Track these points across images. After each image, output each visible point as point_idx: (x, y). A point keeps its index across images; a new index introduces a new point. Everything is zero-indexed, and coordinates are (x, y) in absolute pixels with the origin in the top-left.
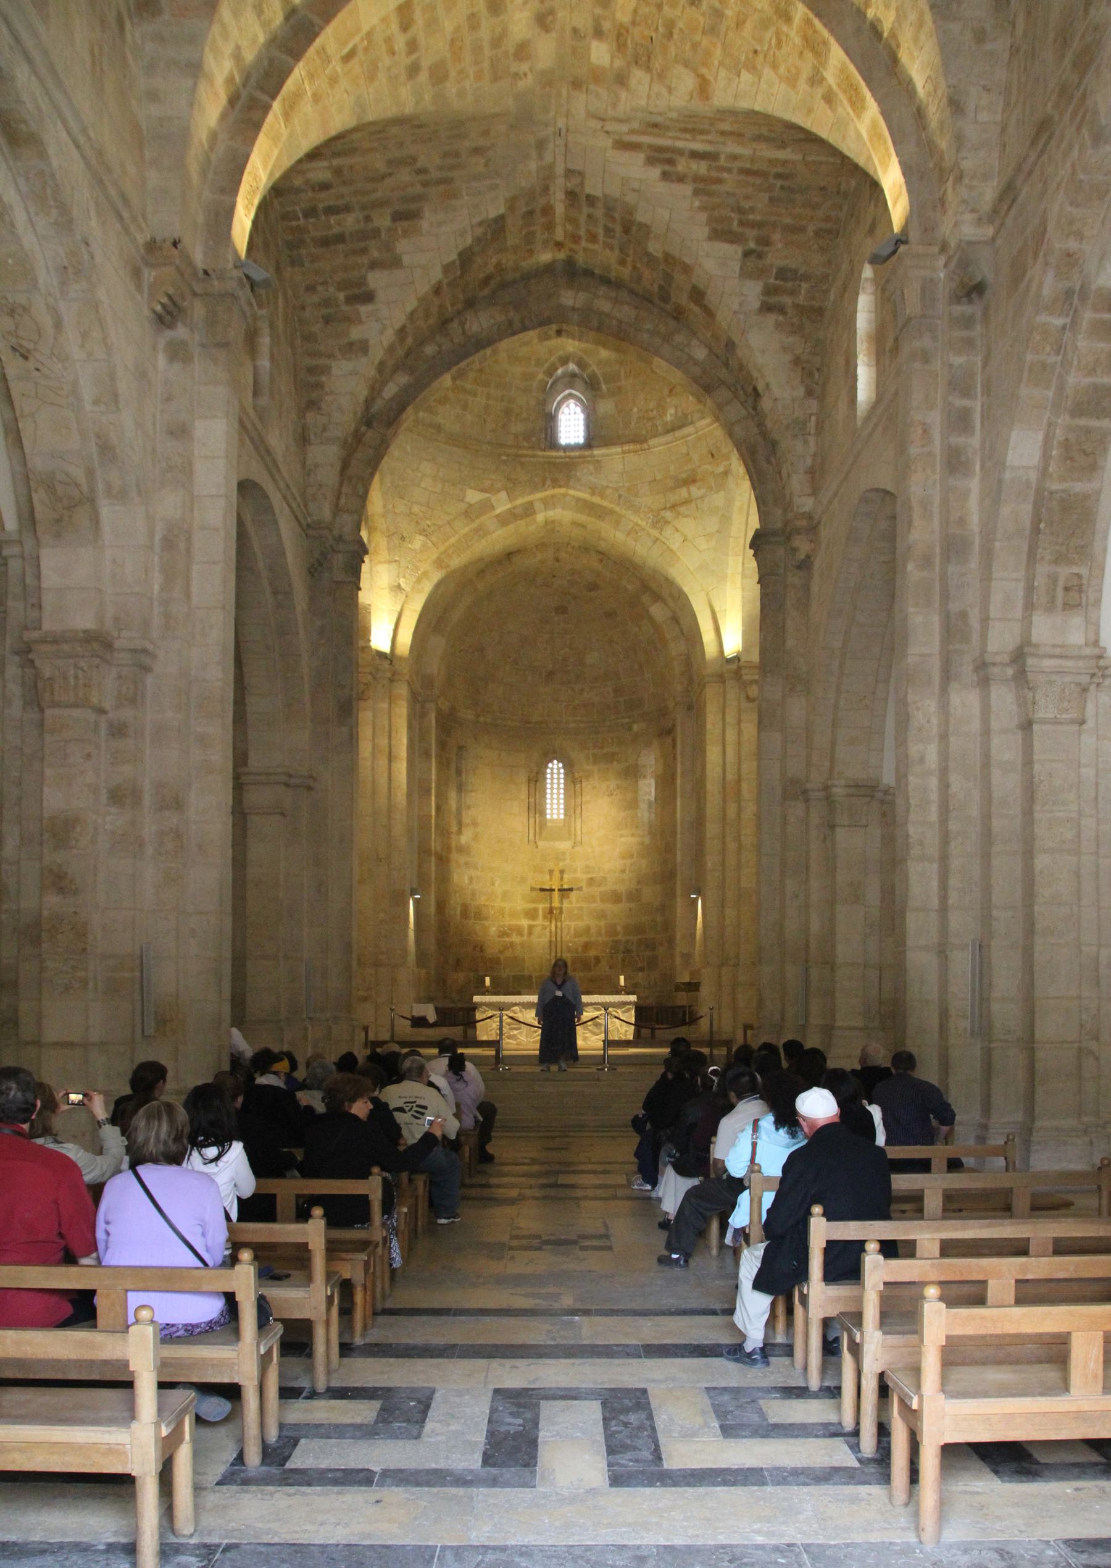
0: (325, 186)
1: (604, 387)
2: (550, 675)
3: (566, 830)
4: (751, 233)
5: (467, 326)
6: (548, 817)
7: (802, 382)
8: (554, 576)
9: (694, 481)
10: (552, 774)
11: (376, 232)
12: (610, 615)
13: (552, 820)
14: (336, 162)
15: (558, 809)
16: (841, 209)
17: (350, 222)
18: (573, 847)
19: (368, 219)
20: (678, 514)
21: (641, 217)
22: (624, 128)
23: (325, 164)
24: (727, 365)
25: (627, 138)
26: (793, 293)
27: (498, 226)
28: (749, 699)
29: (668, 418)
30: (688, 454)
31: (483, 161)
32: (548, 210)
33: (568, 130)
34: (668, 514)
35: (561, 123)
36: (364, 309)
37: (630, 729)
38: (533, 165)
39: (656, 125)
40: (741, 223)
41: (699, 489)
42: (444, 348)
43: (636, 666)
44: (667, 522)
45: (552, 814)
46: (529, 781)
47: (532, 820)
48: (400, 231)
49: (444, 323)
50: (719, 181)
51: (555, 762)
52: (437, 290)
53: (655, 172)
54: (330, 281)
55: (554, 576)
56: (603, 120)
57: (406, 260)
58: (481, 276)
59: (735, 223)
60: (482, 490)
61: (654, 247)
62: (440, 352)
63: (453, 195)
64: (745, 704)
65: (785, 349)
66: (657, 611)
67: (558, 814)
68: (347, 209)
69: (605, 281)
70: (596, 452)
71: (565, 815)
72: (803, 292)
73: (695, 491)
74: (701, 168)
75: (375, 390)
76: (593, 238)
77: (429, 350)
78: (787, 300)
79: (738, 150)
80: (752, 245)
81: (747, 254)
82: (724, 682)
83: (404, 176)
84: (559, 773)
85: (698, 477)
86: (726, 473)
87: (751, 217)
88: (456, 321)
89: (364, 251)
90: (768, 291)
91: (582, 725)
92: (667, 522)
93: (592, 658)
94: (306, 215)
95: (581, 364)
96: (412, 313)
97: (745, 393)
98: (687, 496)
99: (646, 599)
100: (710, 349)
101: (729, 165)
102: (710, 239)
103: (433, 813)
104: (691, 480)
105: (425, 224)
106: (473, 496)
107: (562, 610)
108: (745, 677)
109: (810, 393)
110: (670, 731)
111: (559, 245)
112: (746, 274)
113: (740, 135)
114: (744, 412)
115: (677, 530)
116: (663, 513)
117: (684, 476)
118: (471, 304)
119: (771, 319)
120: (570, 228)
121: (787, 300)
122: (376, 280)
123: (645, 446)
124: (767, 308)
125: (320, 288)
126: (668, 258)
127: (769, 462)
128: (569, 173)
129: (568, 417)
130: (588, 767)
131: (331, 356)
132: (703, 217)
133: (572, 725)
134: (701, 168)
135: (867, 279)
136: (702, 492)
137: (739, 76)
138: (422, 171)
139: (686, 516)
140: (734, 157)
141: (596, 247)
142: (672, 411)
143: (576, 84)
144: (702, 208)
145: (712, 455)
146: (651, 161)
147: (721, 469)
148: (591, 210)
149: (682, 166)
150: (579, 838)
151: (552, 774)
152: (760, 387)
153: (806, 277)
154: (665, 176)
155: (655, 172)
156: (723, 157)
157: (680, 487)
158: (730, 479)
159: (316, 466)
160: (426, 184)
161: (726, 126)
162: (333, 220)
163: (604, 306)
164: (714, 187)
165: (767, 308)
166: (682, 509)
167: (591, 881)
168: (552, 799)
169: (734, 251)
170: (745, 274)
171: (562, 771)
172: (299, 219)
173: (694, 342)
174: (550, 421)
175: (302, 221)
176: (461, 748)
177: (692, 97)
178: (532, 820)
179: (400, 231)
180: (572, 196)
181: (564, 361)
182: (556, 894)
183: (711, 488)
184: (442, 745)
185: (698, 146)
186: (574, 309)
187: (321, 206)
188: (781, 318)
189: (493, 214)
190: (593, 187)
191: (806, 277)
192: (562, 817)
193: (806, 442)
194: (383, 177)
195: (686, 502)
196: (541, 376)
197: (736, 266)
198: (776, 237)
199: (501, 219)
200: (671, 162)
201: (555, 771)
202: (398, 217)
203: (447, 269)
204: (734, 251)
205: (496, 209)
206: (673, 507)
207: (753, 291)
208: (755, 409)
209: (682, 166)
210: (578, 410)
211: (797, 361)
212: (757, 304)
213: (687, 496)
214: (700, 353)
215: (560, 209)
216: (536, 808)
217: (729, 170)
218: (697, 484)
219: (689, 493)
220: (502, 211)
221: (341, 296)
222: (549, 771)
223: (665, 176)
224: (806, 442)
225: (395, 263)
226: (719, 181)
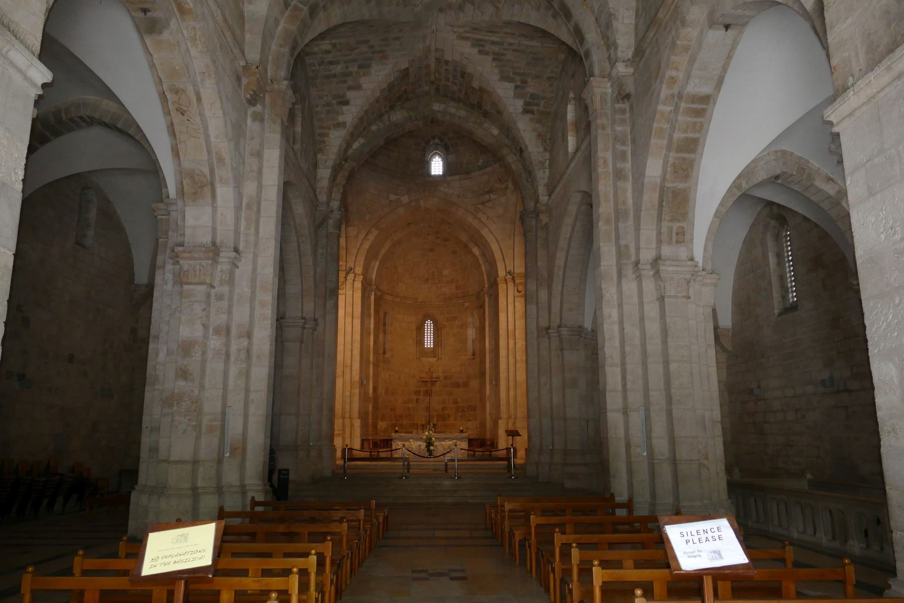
0: (328, 52)
1: (451, 149)
2: (427, 280)
3: (433, 352)
4: (518, 78)
5: (391, 117)
6: (426, 346)
7: (542, 145)
9: (492, 192)
10: (427, 326)
11: (350, 74)
13: (427, 347)
14: (333, 41)
15: (430, 343)
16: (558, 68)
17: (338, 69)
18: (437, 361)
19: (347, 67)
21: (469, 70)
22: (461, 30)
23: (328, 42)
24: (507, 137)
25: (463, 35)
26: (537, 105)
27: (405, 73)
28: (519, 292)
29: (480, 163)
31: (399, 43)
32: (428, 67)
33: (437, 30)
35: (434, 27)
36: (345, 108)
37: (464, 305)
38: (421, 46)
39: (475, 29)
40: (514, 73)
41: (494, 195)
42: (380, 127)
45: (427, 345)
46: (417, 329)
47: (418, 348)
48: (361, 73)
49: (381, 116)
50: (504, 55)
51: (429, 321)
52: (377, 101)
53: (476, 50)
54: (329, 95)
56: (452, 26)
57: (364, 86)
58: (397, 95)
59: (511, 73)
60: (397, 195)
61: (476, 84)
62: (379, 129)
63: (385, 57)
64: (517, 294)
65: (534, 130)
66: (476, 251)
67: (430, 345)
68: (337, 62)
69: (453, 99)
70: (449, 178)
71: (433, 345)
72: (542, 104)
73: (492, 196)
74: (496, 49)
75: (349, 145)
76: (447, 79)
77: (374, 128)
78: (535, 108)
79: (513, 41)
80: (519, 83)
81: (516, 87)
82: (507, 283)
83: (364, 48)
84: (431, 326)
86: (506, 188)
87: (518, 71)
88: (386, 115)
89: (345, 82)
90: (527, 104)
91: (441, 303)
93: (446, 272)
94: (320, 65)
95: (441, 139)
96: (366, 111)
97: (516, 150)
98: (488, 198)
99: (471, 245)
100: (500, 130)
101: (508, 48)
102: (500, 80)
103: (372, 343)
104: (489, 192)
105: (373, 71)
106: (392, 197)
107: (432, 250)
108: (517, 281)
109: (545, 150)
110: (482, 307)
111: (432, 83)
112: (516, 96)
113: (513, 34)
114: (516, 159)
115: (484, 213)
117: (487, 189)
118: (392, 108)
119: (528, 117)
120: (437, 75)
121: (535, 108)
122: (350, 95)
123: (470, 176)
124: (526, 111)
125: (325, 98)
126: (482, 90)
127: (527, 181)
128: (437, 50)
129: (435, 163)
130: (444, 323)
131: (329, 128)
132: (497, 70)
133: (437, 303)
134: (496, 49)
135: (571, 98)
136: (496, 196)
137: (513, 7)
138: (372, 47)
139: (489, 208)
140: (511, 44)
141: (449, 84)
142: (481, 160)
143: (441, 10)
144: (496, 67)
146: (473, 46)
147: (504, 186)
148: (447, 67)
149: (488, 47)
150: (440, 356)
151: (427, 326)
152: (523, 147)
153: (544, 98)
154: (480, 52)
155: (476, 50)
156: (506, 44)
157: (485, 194)
159: (321, 178)
160: (373, 53)
161: (507, 30)
162: (331, 67)
163: (453, 111)
164: (502, 57)
165: (526, 111)
166: (488, 205)
167: (446, 378)
168: (427, 338)
169: (511, 86)
170: (516, 96)
171: (432, 325)
172: (316, 67)
173: (493, 127)
174: (426, 165)
175: (317, 67)
176: (385, 313)
177: (492, 16)
178: (418, 348)
179: (361, 73)
180: (438, 60)
181: (434, 138)
182: (429, 384)
184: (377, 312)
185: (494, 39)
186: (439, 111)
187: (326, 61)
188: (532, 116)
189: (403, 67)
190: (448, 57)
191: (544, 98)
192: (432, 346)
193: (544, 172)
194: (354, 49)
195: (489, 201)
196: (423, 144)
197: (511, 93)
198: (529, 80)
199: (407, 69)
200: (483, 46)
201: (429, 325)
202: (361, 67)
203: (382, 91)
204: (511, 86)
205: (404, 65)
207: (519, 104)
208: (521, 157)
209: (488, 47)
210: (440, 160)
211: (539, 135)
212: (521, 110)
213: (488, 198)
214: (495, 132)
215: (433, 66)
216: (420, 341)
217: (508, 50)
220: (407, 66)
221: (335, 102)
222: (426, 325)
223: (480, 52)
224: (544, 172)
225: (358, 87)
226: (504, 55)
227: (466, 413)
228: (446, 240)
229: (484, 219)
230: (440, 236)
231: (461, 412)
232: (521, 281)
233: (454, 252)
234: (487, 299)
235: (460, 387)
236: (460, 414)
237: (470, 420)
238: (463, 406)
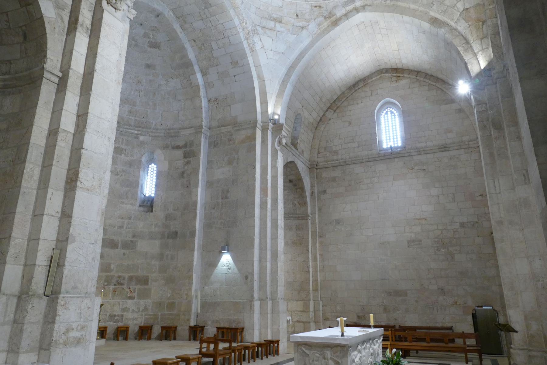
8: (141, 24)
9: (280, 22)
12: (148, 66)
20: (265, 33)
30: (282, 7)
34: (259, 29)
37: (137, 138)
41: (281, 27)
43: (151, 103)
44: (258, 33)
55: (141, 24)
73: (278, 26)
85: (283, 21)
86: (302, 28)
92: (258, 33)
98: (273, 26)
104: (278, 20)
108: (283, 132)
115: (261, 40)
116: (257, 27)
117: (275, 16)
145: (297, 15)
147: (301, 24)
158: (305, 31)
166: (268, 31)
183: (288, 30)
206: (264, 28)
213: (273, 26)
218: (281, 24)
219: (275, 26)
227: (125, 287)
228: (155, 45)
229: (258, 46)
230: (151, 36)
231: (115, 285)
232: (286, 135)
233: (148, 66)
234: (203, 140)
235: (117, 248)
236: (112, 287)
237: (131, 298)
238: (119, 277)
